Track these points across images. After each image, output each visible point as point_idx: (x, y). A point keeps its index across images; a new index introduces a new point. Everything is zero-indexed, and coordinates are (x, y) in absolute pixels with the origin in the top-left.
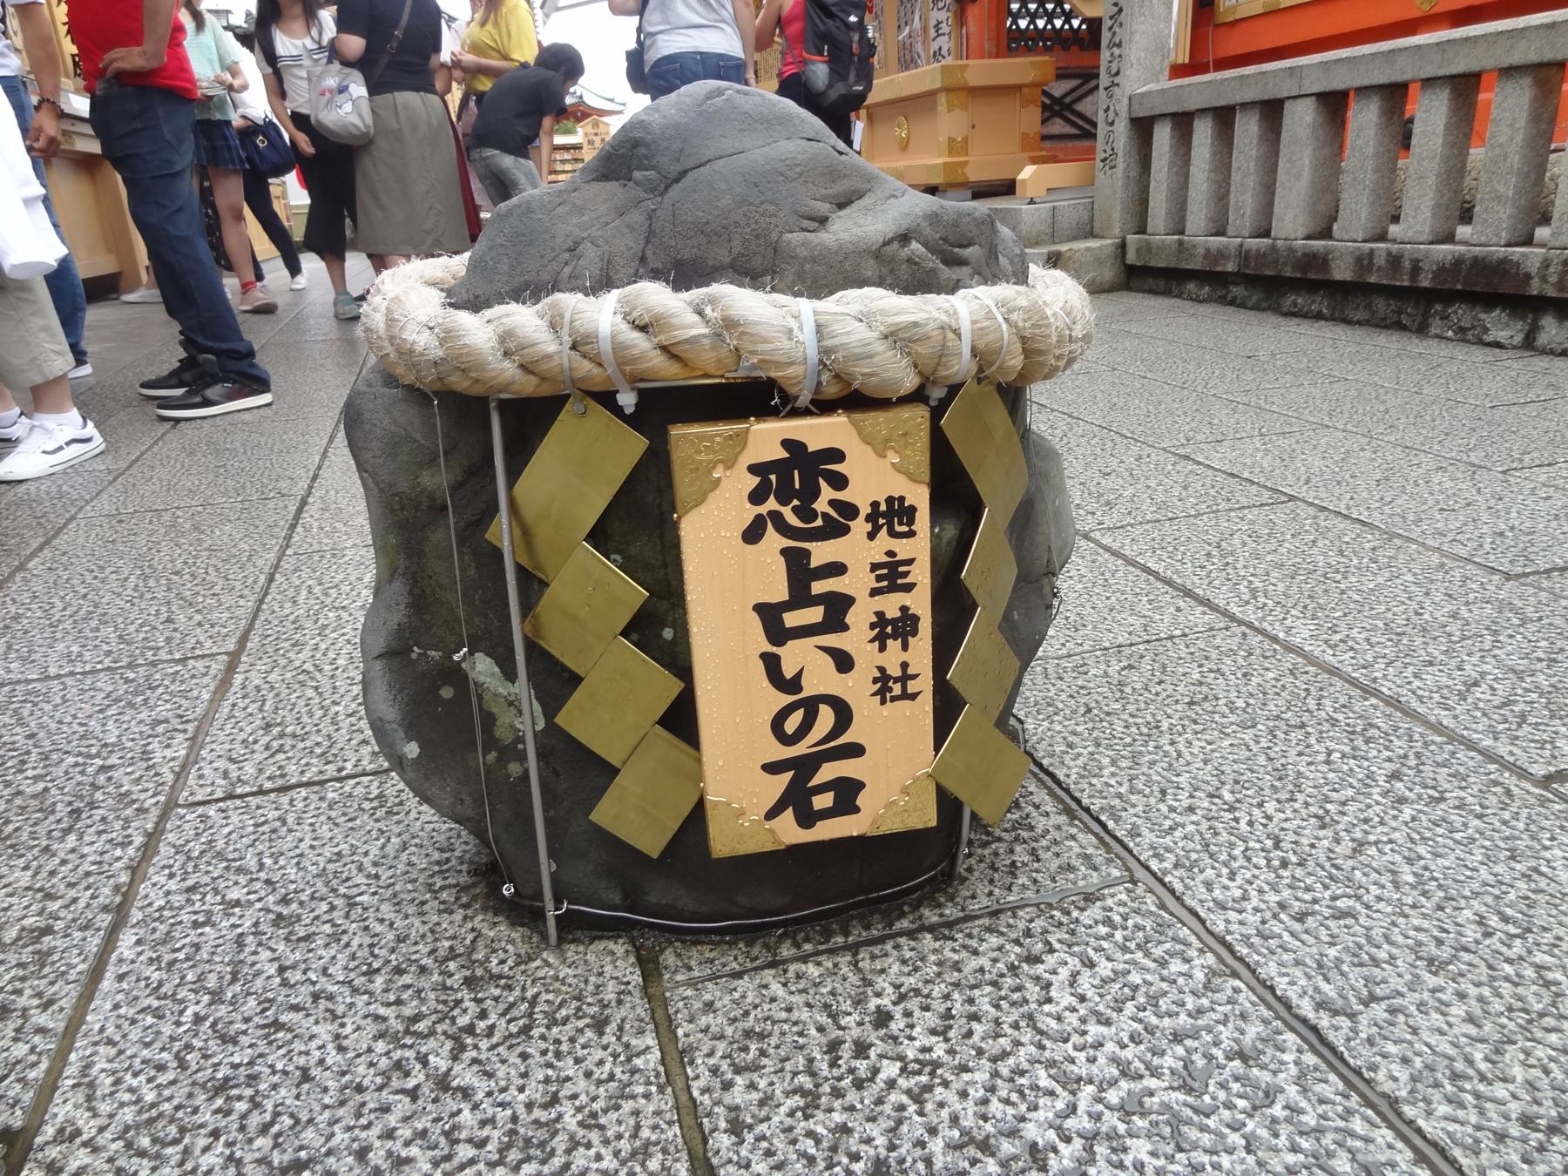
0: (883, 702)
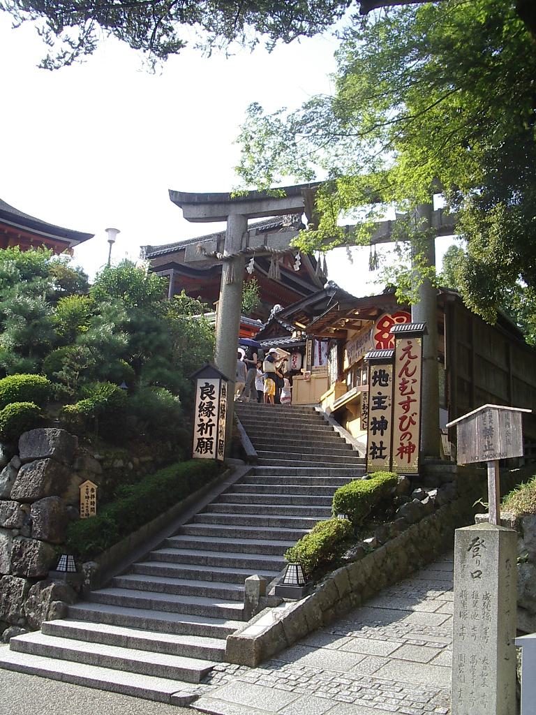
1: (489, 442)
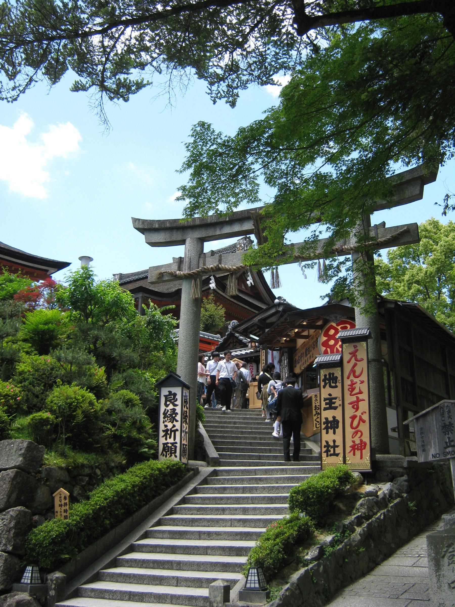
0: (327, 456)
1: (449, 438)
